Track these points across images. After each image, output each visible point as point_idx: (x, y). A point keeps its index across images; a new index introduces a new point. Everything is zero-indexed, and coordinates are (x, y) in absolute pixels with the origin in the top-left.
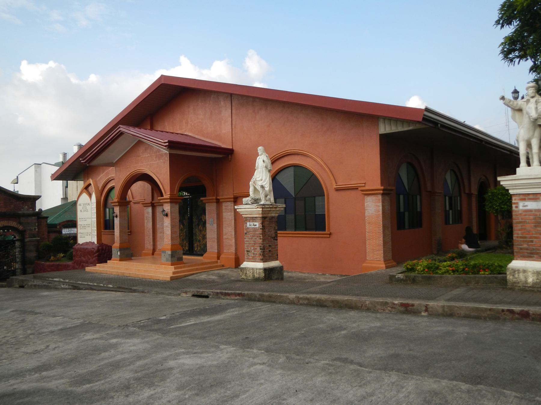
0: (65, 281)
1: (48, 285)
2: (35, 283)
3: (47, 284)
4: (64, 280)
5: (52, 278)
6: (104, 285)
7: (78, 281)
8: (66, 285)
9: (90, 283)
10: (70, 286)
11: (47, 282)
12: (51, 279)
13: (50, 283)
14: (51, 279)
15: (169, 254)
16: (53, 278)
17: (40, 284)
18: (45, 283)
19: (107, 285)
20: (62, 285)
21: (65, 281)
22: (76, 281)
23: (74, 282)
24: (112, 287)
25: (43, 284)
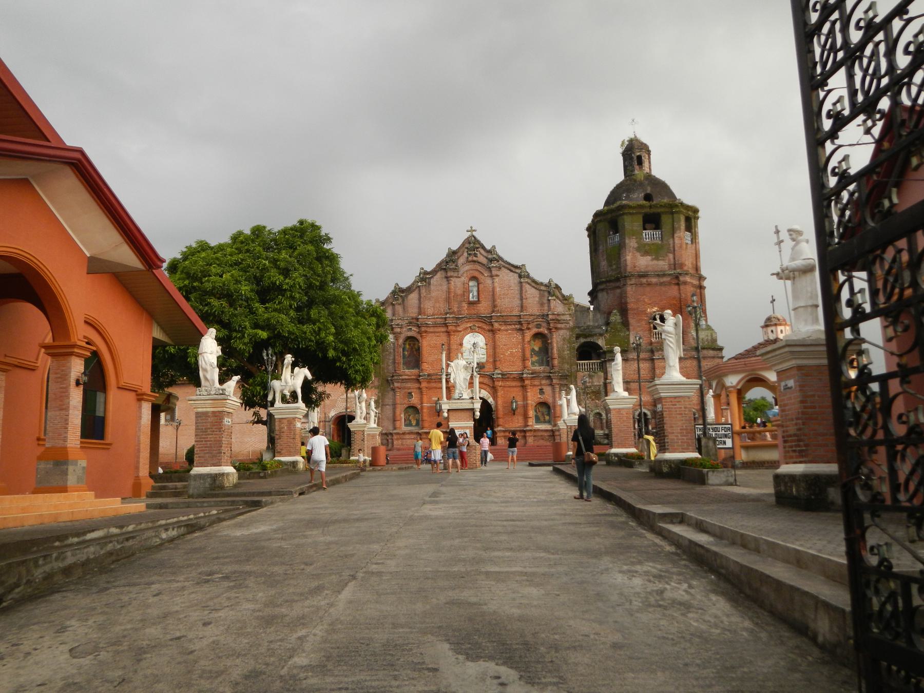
0: (124, 530)
1: (123, 547)
2: (70, 559)
3: (119, 547)
4: (121, 527)
5: (78, 535)
6: (204, 513)
7: (158, 521)
8: (173, 529)
9: (183, 517)
10: (182, 528)
11: (118, 542)
12: (76, 540)
13: (127, 539)
14: (76, 540)
15: (84, 468)
16: (85, 533)
17: (92, 557)
18: (110, 545)
19: (209, 512)
20: (163, 531)
21: (124, 530)
22: (152, 522)
23: (150, 525)
24: (216, 514)
25: (102, 552)
